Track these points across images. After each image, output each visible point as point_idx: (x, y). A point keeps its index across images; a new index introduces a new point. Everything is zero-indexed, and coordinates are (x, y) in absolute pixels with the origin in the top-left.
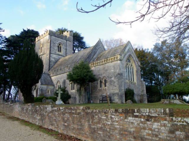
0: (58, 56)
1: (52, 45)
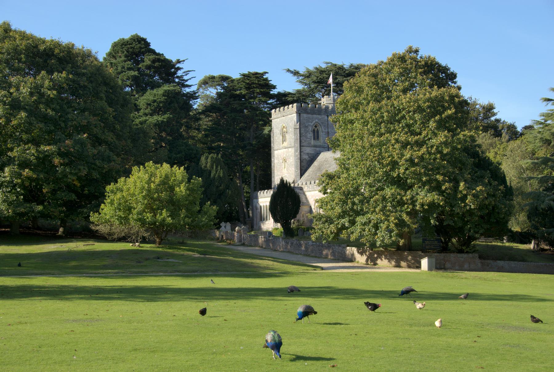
0: (315, 148)
1: (302, 132)
